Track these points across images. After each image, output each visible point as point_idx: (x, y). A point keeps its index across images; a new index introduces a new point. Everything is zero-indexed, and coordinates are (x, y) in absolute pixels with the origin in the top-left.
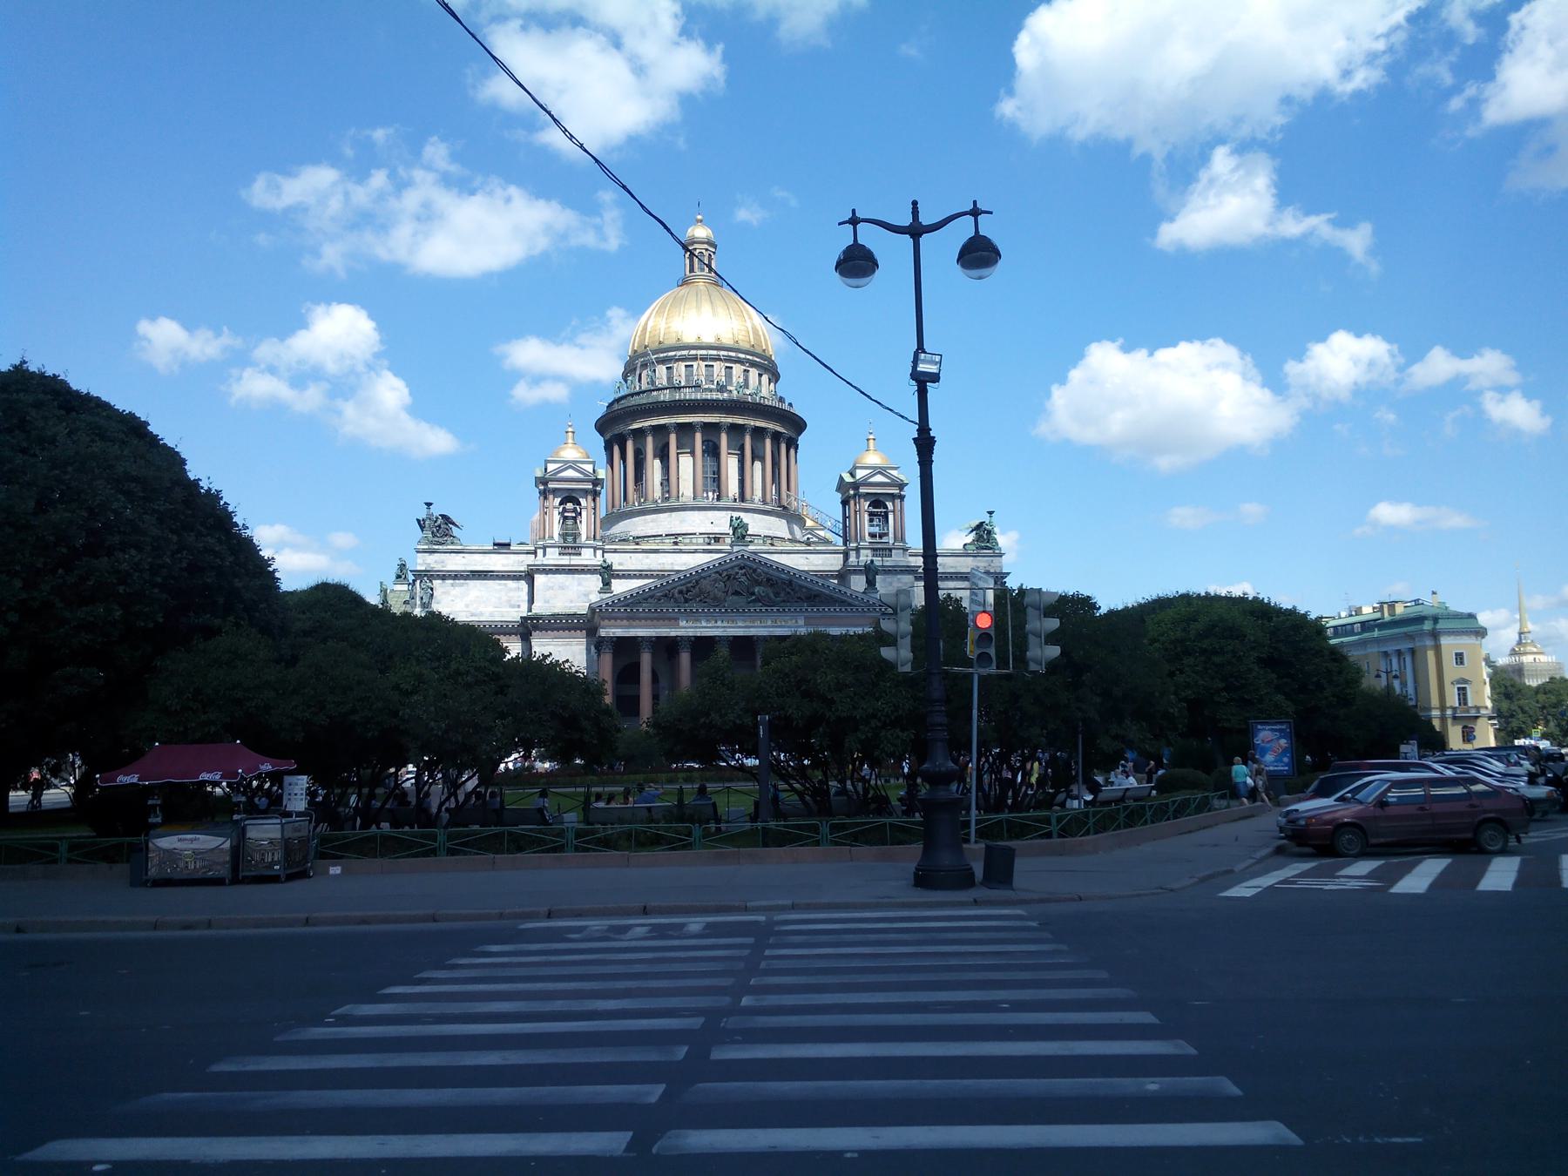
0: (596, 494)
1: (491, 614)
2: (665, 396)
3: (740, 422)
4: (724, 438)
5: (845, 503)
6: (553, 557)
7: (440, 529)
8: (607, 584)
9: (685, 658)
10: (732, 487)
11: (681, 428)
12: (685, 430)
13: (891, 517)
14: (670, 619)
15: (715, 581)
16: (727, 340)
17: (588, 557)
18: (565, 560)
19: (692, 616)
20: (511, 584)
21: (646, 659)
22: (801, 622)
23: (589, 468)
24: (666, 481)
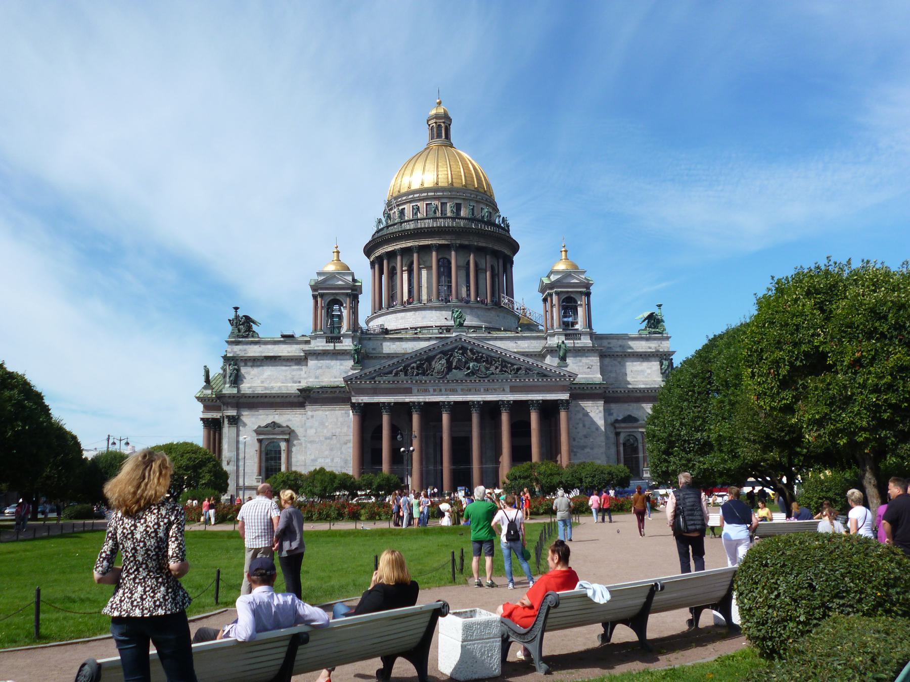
1: (280, 387)
2: (411, 226)
3: (467, 243)
5: (545, 300)
6: (320, 344)
7: (244, 327)
8: (357, 362)
13: (580, 310)
18: (330, 347)
22: (508, 389)
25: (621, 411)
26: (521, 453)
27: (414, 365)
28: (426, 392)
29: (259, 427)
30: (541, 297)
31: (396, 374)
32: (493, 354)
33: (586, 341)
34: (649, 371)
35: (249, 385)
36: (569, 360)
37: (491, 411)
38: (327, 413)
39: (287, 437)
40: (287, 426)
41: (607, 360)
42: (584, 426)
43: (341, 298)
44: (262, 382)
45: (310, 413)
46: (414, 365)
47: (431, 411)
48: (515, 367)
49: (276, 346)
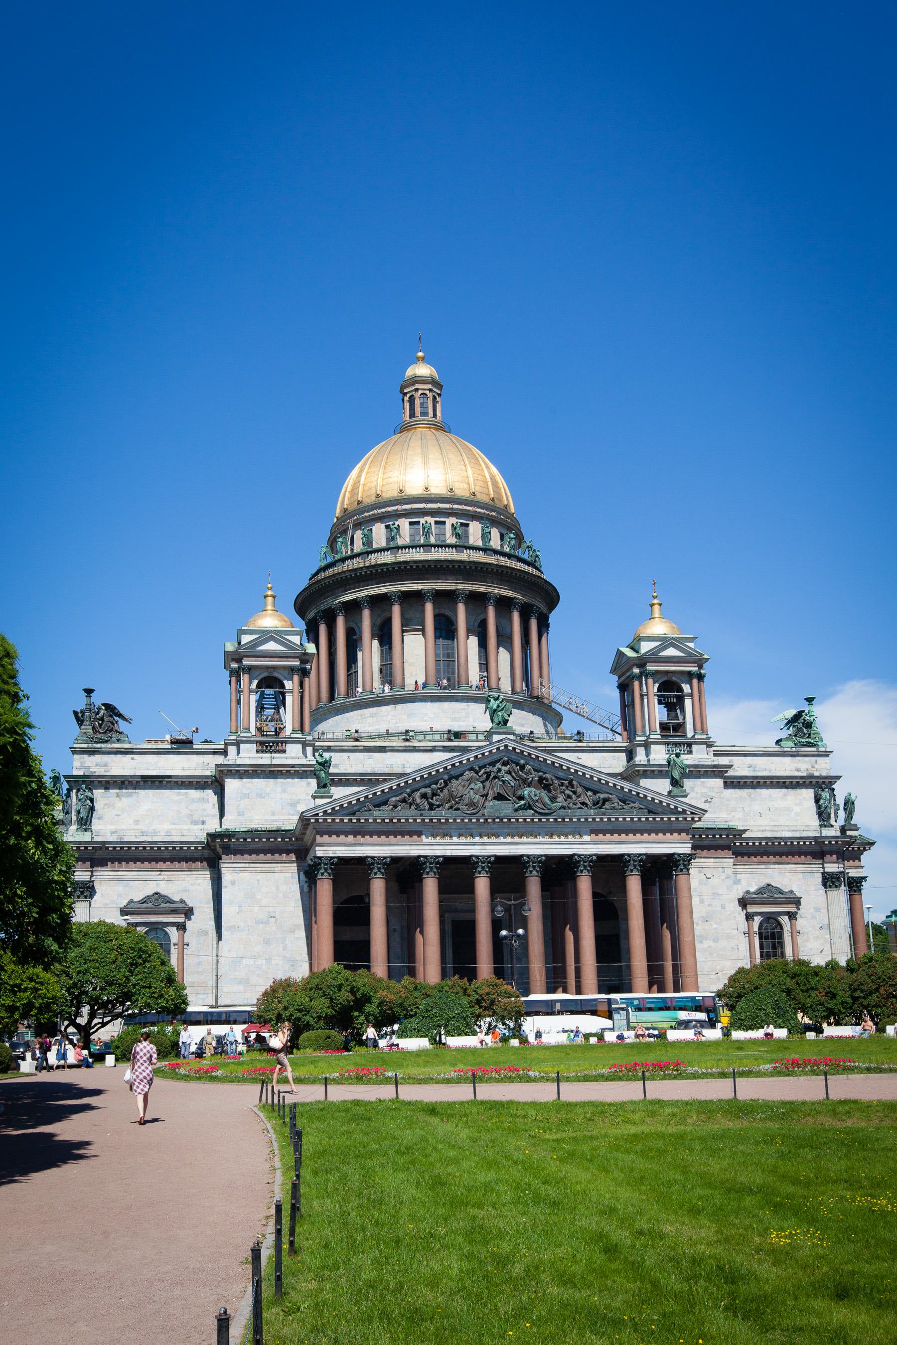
0: (304, 673)
1: (168, 833)
2: (386, 558)
3: (481, 588)
4: (461, 608)
5: (624, 687)
6: (249, 755)
9: (430, 887)
10: (474, 674)
11: (408, 598)
12: (412, 600)
13: (688, 702)
14: (411, 834)
15: (470, 781)
16: (462, 491)
17: (293, 755)
18: (265, 759)
19: (441, 830)
20: (194, 794)
21: (378, 887)
23: (296, 639)
25: (753, 877)
26: (611, 948)
27: (428, 790)
29: (131, 901)
30: (614, 680)
31: (395, 807)
32: (561, 774)
33: (700, 756)
34: (797, 809)
35: (113, 827)
36: (688, 784)
37: (559, 872)
38: (259, 876)
39: (180, 919)
40: (182, 901)
41: (730, 792)
42: (702, 901)
44: (137, 822)
45: (227, 878)
46: (428, 790)
47: (456, 873)
48: (602, 796)
49: (163, 757)
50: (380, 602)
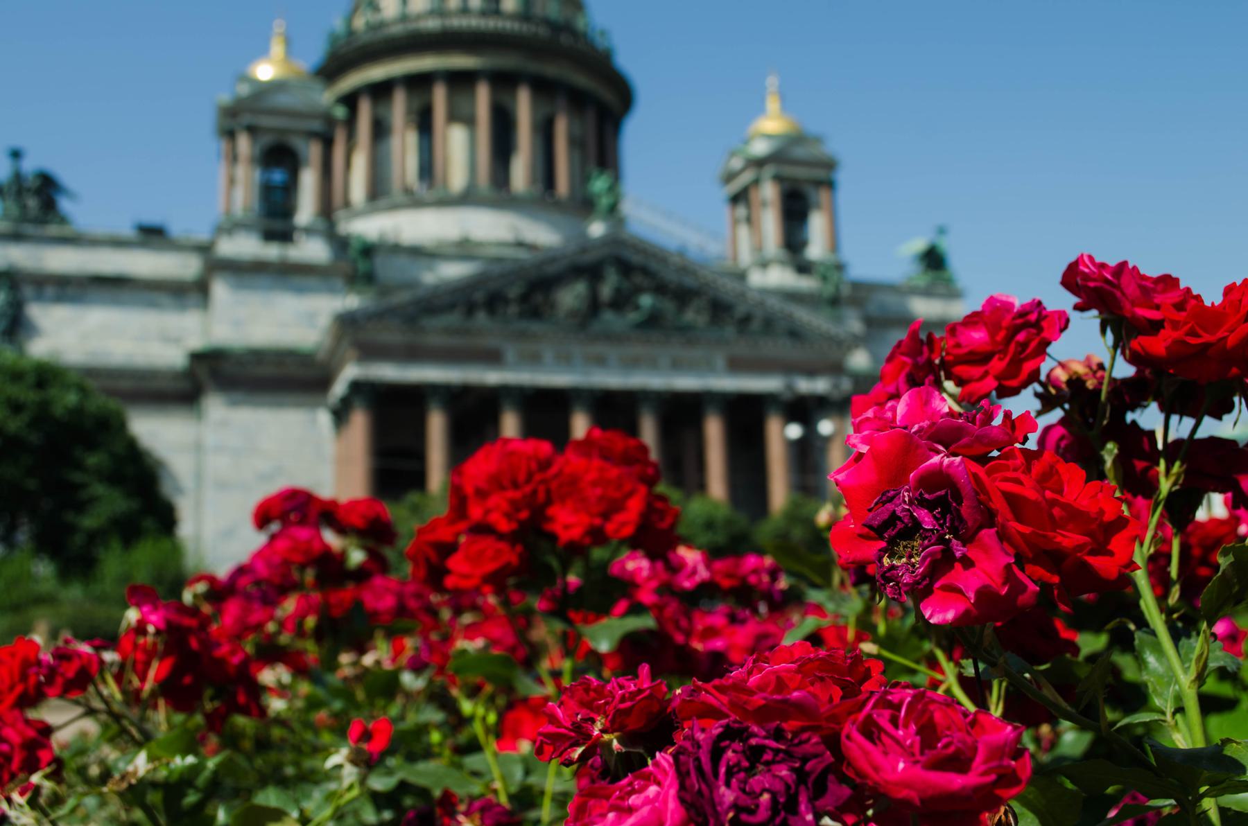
6: (245, 246)
12: (460, 81)
17: (313, 250)
18: (272, 252)
22: (720, 361)
24: (427, 169)
28: (534, 360)
43: (298, 143)
50: (419, 83)
